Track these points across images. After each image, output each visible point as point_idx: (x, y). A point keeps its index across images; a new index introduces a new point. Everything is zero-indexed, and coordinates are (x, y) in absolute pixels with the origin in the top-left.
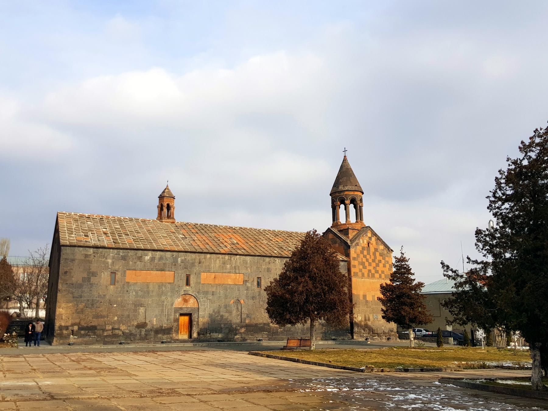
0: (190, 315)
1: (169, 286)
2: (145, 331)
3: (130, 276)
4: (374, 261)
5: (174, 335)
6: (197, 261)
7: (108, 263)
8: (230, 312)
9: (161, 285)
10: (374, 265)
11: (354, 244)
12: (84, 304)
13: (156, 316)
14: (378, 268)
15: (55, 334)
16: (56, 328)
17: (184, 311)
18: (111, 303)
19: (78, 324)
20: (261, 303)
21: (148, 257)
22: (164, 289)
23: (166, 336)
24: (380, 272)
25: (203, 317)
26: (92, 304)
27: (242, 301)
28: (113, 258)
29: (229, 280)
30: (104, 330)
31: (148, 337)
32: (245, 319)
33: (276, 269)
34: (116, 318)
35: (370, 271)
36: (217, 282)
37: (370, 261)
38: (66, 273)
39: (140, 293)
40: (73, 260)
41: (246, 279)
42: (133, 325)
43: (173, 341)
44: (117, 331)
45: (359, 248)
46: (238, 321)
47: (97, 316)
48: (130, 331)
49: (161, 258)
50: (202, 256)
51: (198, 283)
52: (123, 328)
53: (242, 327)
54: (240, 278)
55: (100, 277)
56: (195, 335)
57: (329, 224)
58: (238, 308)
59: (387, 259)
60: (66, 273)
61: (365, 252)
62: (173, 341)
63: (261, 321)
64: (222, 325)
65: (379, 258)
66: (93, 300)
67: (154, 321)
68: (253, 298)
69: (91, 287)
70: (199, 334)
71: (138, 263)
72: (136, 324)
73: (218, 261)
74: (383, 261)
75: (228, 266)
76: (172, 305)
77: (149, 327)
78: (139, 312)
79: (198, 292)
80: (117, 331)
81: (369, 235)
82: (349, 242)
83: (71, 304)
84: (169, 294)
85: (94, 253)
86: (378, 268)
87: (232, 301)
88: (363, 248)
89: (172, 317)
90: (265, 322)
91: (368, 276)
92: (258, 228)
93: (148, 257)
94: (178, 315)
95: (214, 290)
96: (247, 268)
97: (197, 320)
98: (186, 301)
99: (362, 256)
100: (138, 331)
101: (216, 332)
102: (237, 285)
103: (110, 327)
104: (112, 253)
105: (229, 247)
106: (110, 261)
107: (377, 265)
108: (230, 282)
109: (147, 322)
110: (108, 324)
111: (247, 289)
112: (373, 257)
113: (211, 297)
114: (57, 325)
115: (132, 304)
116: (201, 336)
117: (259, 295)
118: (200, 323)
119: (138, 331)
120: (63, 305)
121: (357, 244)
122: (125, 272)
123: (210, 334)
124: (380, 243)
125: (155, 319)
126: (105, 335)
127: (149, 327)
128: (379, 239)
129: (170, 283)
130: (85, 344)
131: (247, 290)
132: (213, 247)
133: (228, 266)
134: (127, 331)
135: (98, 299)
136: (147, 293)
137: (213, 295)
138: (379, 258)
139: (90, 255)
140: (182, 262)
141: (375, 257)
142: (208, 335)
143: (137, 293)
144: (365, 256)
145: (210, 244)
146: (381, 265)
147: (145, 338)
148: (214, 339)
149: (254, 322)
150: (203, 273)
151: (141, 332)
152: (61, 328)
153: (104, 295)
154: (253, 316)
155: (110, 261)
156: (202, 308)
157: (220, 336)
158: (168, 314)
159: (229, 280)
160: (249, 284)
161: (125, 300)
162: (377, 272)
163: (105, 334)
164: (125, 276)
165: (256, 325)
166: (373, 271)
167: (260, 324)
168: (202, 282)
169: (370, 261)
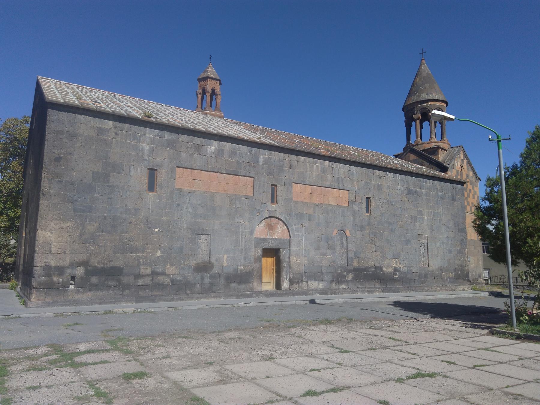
2: (212, 277)
3: (183, 179)
5: (255, 284)
6: (287, 163)
7: (142, 150)
8: (331, 247)
9: (234, 199)
12: (96, 225)
15: (34, 284)
17: (270, 245)
19: (84, 264)
20: (372, 236)
21: (213, 147)
22: (238, 205)
23: (243, 286)
25: (297, 255)
27: (348, 233)
28: (152, 142)
29: (331, 199)
30: (137, 276)
32: (352, 260)
33: (388, 187)
34: (159, 254)
36: (315, 200)
38: (58, 159)
40: (73, 136)
42: (190, 266)
43: (254, 295)
44: (161, 278)
46: (343, 262)
49: (233, 153)
50: (294, 157)
51: (289, 200)
52: (172, 271)
53: (349, 271)
54: (343, 196)
56: (286, 285)
58: (342, 243)
60: (58, 159)
62: (254, 295)
63: (372, 264)
64: (324, 270)
67: (225, 260)
68: (362, 228)
70: (291, 282)
71: (196, 156)
72: (193, 263)
73: (315, 167)
74: (472, 191)
76: (252, 233)
77: (216, 270)
79: (290, 215)
80: (161, 278)
83: (69, 224)
85: (116, 127)
87: (336, 231)
88: (458, 172)
89: (252, 254)
90: (377, 265)
93: (213, 148)
94: (260, 252)
96: (353, 183)
97: (287, 259)
98: (271, 228)
100: (198, 277)
102: (340, 206)
103: (149, 271)
104: (150, 133)
106: (146, 147)
108: (332, 202)
109: (213, 260)
110: (144, 265)
114: (39, 264)
117: (369, 224)
118: (294, 266)
119: (198, 277)
120: (53, 225)
122: (173, 171)
123: (307, 282)
124: (470, 168)
125: (225, 257)
126: (139, 284)
127: (216, 270)
129: (247, 197)
130: (100, 303)
131: (354, 215)
133: (329, 177)
134: (179, 278)
137: (309, 220)
139: (108, 130)
142: (305, 283)
147: (209, 290)
148: (313, 290)
149: (364, 264)
150: (294, 185)
151: (202, 278)
152: (48, 270)
154: (362, 256)
155: (146, 147)
156: (294, 240)
157: (321, 285)
159: (331, 199)
160: (356, 207)
163: (140, 282)
165: (366, 269)
167: (371, 267)
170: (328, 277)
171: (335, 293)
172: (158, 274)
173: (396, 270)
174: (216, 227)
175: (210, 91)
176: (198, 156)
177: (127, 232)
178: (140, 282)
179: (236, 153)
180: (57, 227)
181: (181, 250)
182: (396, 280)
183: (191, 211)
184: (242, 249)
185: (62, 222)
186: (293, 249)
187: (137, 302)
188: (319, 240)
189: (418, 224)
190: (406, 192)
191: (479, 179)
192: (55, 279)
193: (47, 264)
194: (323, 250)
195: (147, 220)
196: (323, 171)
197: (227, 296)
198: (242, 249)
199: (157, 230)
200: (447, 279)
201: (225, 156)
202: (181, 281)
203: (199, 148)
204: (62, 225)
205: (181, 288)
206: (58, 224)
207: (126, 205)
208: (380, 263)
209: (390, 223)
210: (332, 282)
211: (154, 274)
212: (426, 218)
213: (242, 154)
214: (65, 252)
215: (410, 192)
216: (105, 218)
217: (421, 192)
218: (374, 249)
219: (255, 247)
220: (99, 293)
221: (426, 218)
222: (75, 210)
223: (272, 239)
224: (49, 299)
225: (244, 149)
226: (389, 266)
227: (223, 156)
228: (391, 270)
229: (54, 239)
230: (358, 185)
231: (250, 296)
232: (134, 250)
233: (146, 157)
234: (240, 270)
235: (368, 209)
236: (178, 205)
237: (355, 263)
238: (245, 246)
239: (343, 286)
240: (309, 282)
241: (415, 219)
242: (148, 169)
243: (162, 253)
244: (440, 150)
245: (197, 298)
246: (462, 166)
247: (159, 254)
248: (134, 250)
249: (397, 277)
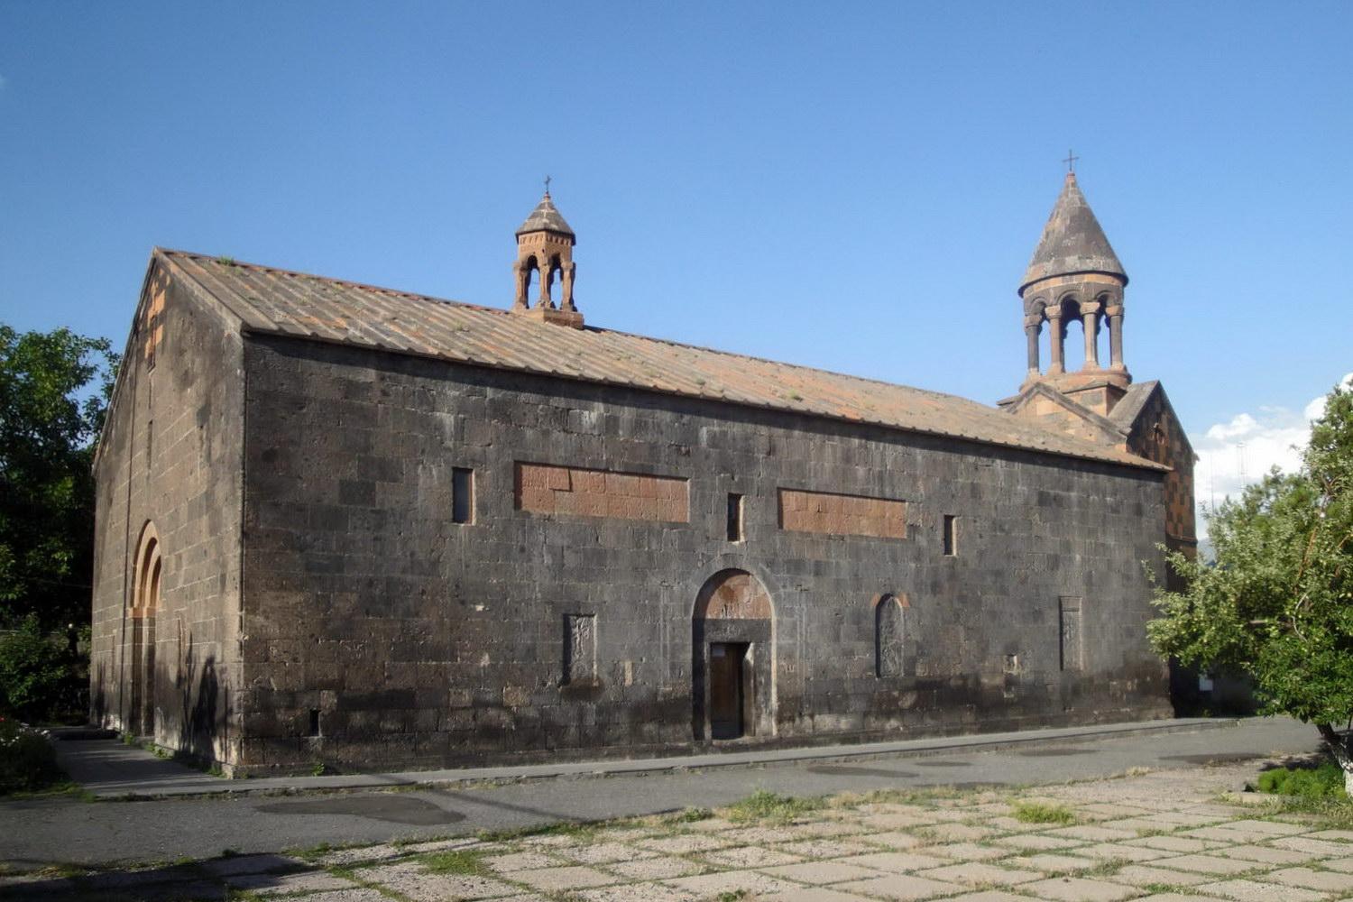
2: (600, 711)
9: (642, 532)
12: (354, 598)
13: (632, 653)
18: (462, 597)
20: (957, 605)
21: (592, 414)
26: (384, 598)
29: (864, 522)
34: (485, 661)
39: (571, 560)
44: (492, 712)
47: (409, 650)
48: (542, 713)
49: (639, 426)
53: (905, 691)
55: (413, 485)
64: (848, 686)
66: (390, 583)
68: (936, 588)
69: (379, 527)
71: (557, 435)
73: (828, 450)
75: (861, 471)
83: (299, 598)
84: (674, 566)
95: (820, 554)
96: (914, 478)
100: (573, 712)
101: (831, 711)
103: (467, 697)
111: (918, 558)
113: (810, 581)
116: (787, 725)
123: (812, 716)
127: (611, 695)
129: (673, 526)
131: (918, 558)
133: (861, 471)
134: (532, 713)
135: (409, 578)
136: (596, 561)
137: (817, 574)
140: (714, 441)
142: (807, 720)
143: (558, 554)
147: (594, 743)
151: (581, 716)
158: (674, 646)
159: (864, 522)
160: (922, 541)
161: (519, 587)
163: (451, 724)
170: (858, 705)
171: (875, 740)
172: (487, 705)
173: (1010, 682)
174: (606, 598)
176: (562, 434)
177: (417, 614)
179: (646, 423)
180: (276, 604)
181: (531, 652)
182: (1010, 704)
183: (550, 562)
184: (665, 646)
185: (284, 594)
188: (838, 618)
189: (1060, 573)
190: (1034, 500)
193: (263, 685)
194: (845, 643)
195: (457, 586)
196: (847, 459)
197: (637, 754)
198: (665, 646)
199: (480, 608)
200: (1121, 696)
201: (621, 433)
202: (536, 720)
203: (563, 419)
204: (285, 600)
206: (277, 598)
207: (412, 554)
208: (973, 667)
209: (998, 574)
210: (866, 714)
211: (478, 704)
212: (1078, 557)
213: (659, 426)
214: (295, 660)
215: (1043, 500)
216: (371, 583)
217: (1069, 497)
218: (962, 635)
221: (1078, 557)
222: (309, 568)
223: (733, 621)
225: (666, 416)
226: (994, 672)
227: (616, 433)
228: (999, 681)
234: (664, 695)
236: (522, 550)
238: (673, 638)
240: (817, 717)
241: (1054, 562)
243: (491, 658)
245: (573, 759)
247: (485, 661)
249: (1012, 696)
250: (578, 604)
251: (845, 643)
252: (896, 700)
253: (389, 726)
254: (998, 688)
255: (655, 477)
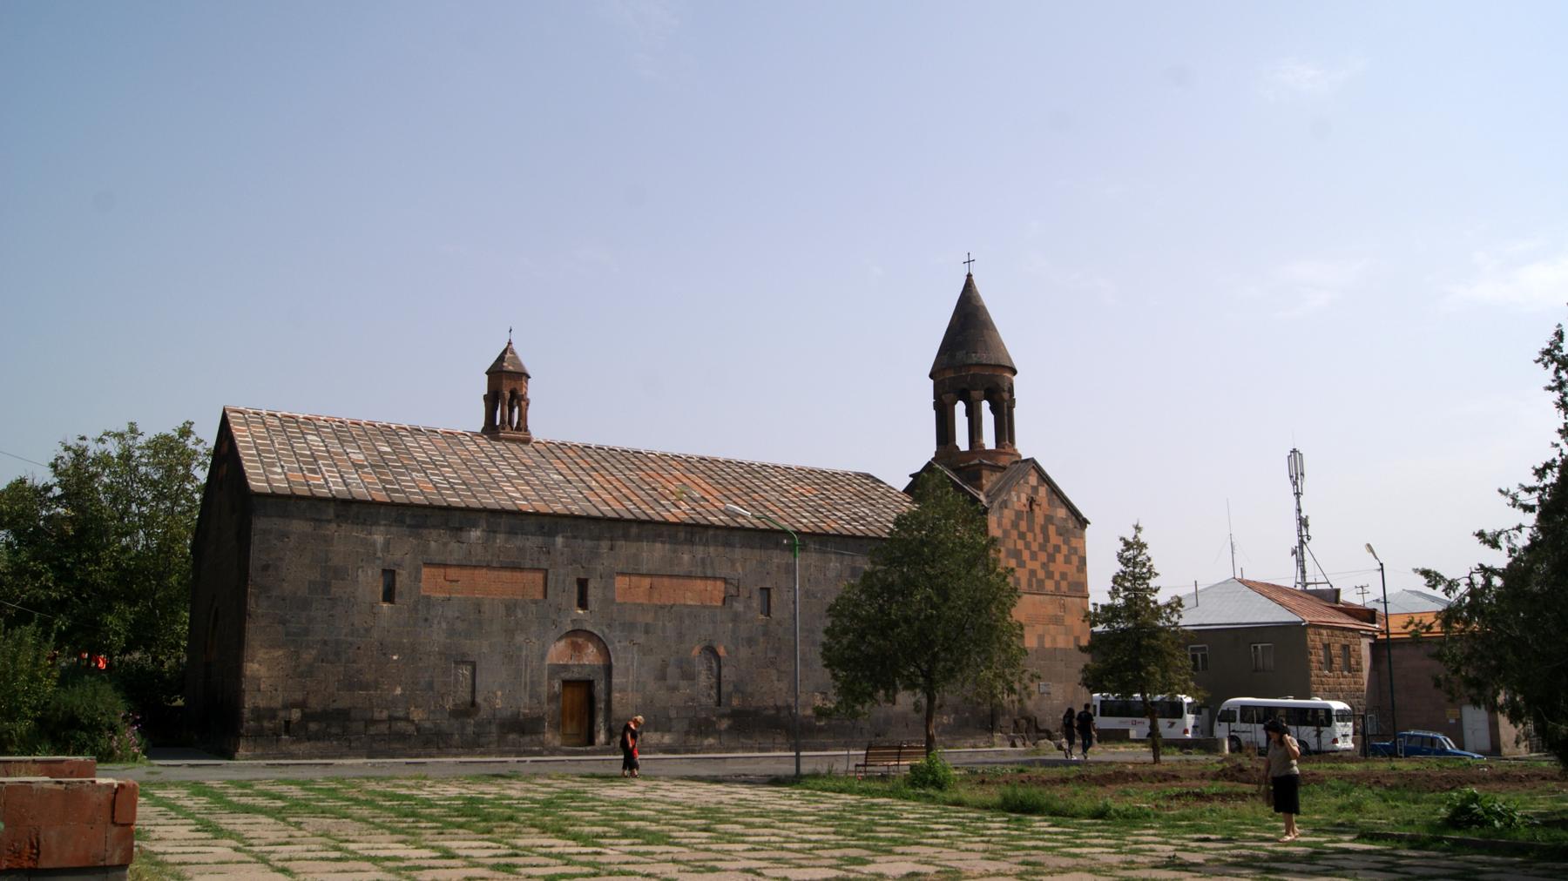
0: (589, 685)
1: (533, 608)
2: (477, 725)
3: (431, 583)
4: (1043, 547)
7: (374, 544)
8: (689, 676)
9: (510, 608)
10: (1043, 557)
11: (996, 504)
12: (314, 652)
14: (1052, 567)
16: (247, 713)
17: (575, 675)
20: (771, 654)
22: (520, 615)
23: (527, 739)
24: (1057, 576)
25: (623, 690)
27: (722, 651)
31: (483, 740)
32: (730, 696)
34: (398, 691)
35: (1033, 573)
37: (1035, 547)
38: (266, 568)
39: (459, 625)
40: (284, 535)
41: (733, 591)
44: (401, 725)
45: (1008, 514)
46: (711, 702)
47: (351, 685)
51: (608, 601)
52: (417, 715)
53: (723, 716)
56: (601, 737)
57: (926, 449)
59: (1074, 542)
60: (266, 568)
61: (1023, 526)
64: (673, 714)
65: (1055, 539)
68: (750, 641)
70: (610, 733)
71: (454, 545)
72: (449, 706)
74: (1065, 549)
76: (543, 657)
77: (483, 714)
78: (456, 675)
79: (609, 626)
80: (401, 725)
81: (1033, 480)
82: (982, 497)
86: (1052, 567)
87: (696, 651)
88: (1019, 514)
89: (544, 690)
90: (779, 703)
91: (1030, 585)
92: (746, 458)
94: (557, 686)
95: (649, 618)
98: (577, 648)
99: (1014, 533)
101: (656, 730)
102: (705, 607)
103: (385, 714)
105: (684, 507)
107: (1051, 558)
109: (479, 700)
111: (736, 618)
112: (1040, 539)
113: (640, 638)
115: (440, 653)
117: (765, 634)
120: (261, 654)
121: (1004, 505)
122: (418, 571)
124: (1058, 502)
127: (483, 714)
128: (1054, 490)
129: (535, 602)
132: (644, 507)
134: (428, 725)
137: (647, 632)
138: (1055, 539)
141: (1047, 539)
144: (1022, 536)
145: (634, 498)
146: (1060, 558)
147: (472, 745)
150: (618, 579)
151: (463, 728)
152: (258, 714)
153: (367, 630)
154: (749, 689)
157: (667, 739)
160: (739, 607)
162: (1050, 575)
164: (418, 579)
166: (1041, 574)
168: (618, 600)
169: (1035, 547)
175: (507, 395)
178: (373, 730)
181: (430, 685)
182: (821, 730)
186: (616, 680)
187: (369, 757)
188: (665, 665)
191: (1084, 523)
192: (266, 724)
194: (670, 682)
205: (431, 741)
210: (687, 733)
211: (391, 719)
216: (325, 643)
219: (550, 678)
220: (320, 744)
222: (287, 634)
224: (259, 751)
226: (804, 707)
229: (263, 672)
230: (744, 568)
231: (539, 754)
232: (365, 686)
233: (379, 554)
235: (767, 611)
237: (735, 702)
239: (711, 741)
242: (384, 571)
244: (985, 473)
246: (1032, 501)
247: (398, 691)
248: (365, 686)
250: (463, 654)
251: (670, 682)
252: (714, 723)
253: (333, 731)
254: (805, 717)
255: (522, 569)
